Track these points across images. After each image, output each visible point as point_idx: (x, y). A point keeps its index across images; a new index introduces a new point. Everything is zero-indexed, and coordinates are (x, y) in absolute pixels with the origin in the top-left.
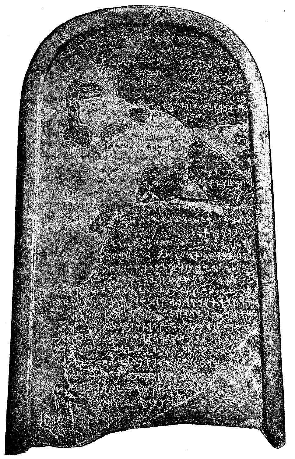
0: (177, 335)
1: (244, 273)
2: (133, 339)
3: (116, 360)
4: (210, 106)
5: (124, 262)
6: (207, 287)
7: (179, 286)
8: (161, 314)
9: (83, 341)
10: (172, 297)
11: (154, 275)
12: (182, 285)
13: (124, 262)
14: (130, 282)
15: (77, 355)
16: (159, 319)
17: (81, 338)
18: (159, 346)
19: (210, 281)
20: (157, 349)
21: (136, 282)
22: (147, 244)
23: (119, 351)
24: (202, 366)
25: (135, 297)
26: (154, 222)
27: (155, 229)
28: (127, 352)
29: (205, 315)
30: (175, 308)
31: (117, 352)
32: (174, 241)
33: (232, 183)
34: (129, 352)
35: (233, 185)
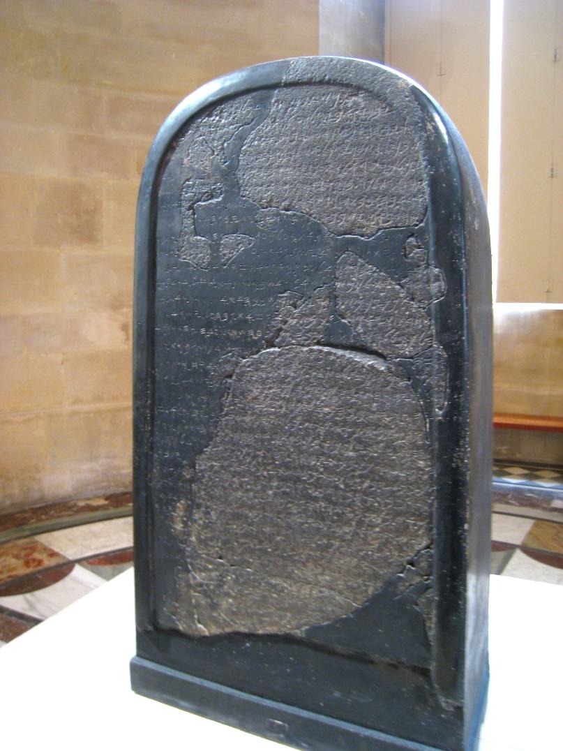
0: (317, 537)
1: (415, 462)
2: (262, 531)
3: (242, 554)
4: (368, 201)
5: (252, 431)
6: (361, 476)
7: (322, 470)
8: (297, 505)
9: (204, 522)
10: (311, 484)
11: (288, 450)
12: (326, 469)
13: (252, 431)
14: (258, 456)
15: (200, 541)
16: (295, 511)
17: (201, 519)
18: (294, 547)
19: (364, 468)
20: (292, 550)
21: (264, 457)
22: (281, 407)
23: (246, 543)
24: (349, 584)
25: (264, 477)
26: (288, 376)
27: (291, 387)
28: (255, 545)
29: (357, 515)
30: (315, 499)
31: (242, 544)
32: (315, 405)
33: (402, 322)
34: (258, 547)
35: (403, 324)
